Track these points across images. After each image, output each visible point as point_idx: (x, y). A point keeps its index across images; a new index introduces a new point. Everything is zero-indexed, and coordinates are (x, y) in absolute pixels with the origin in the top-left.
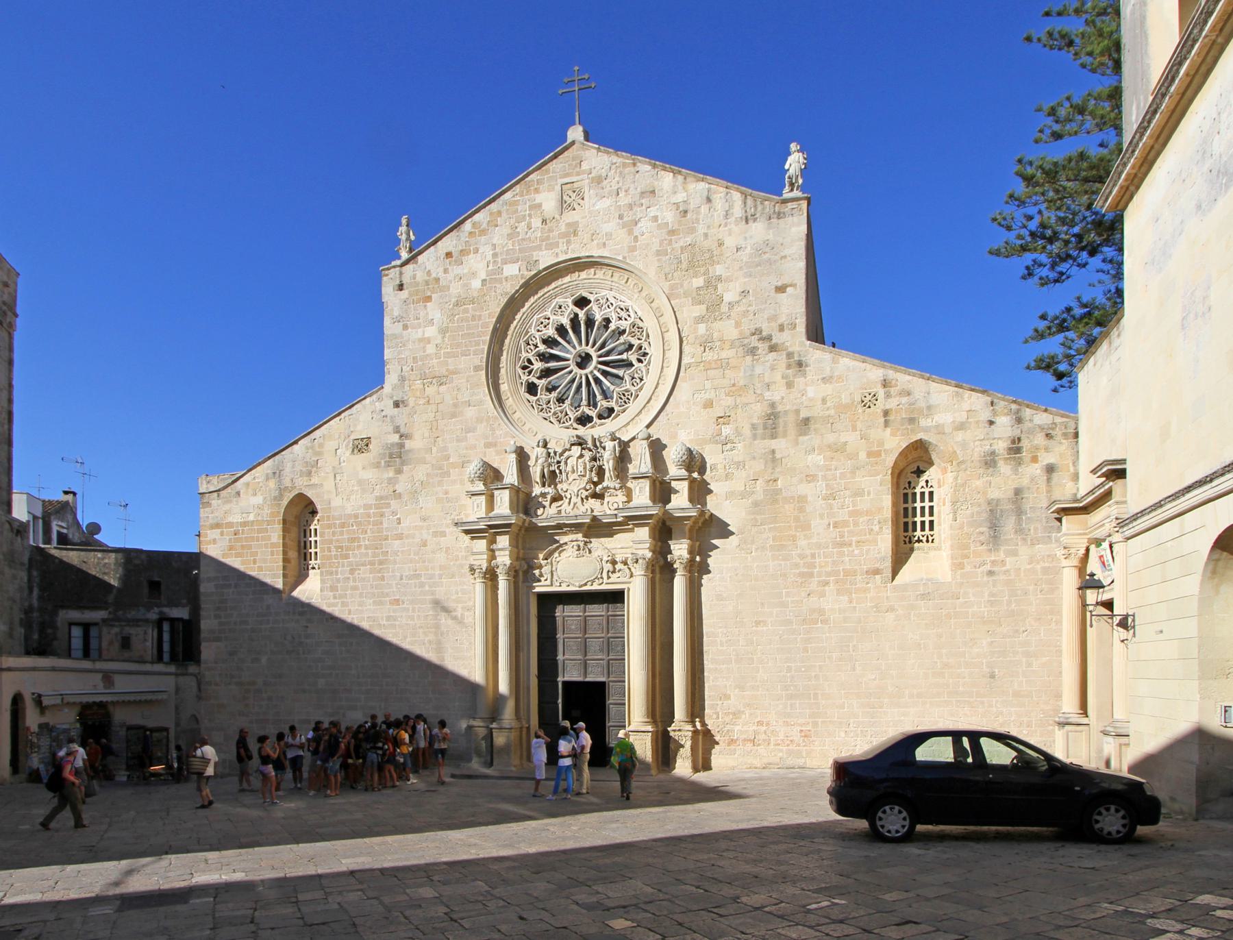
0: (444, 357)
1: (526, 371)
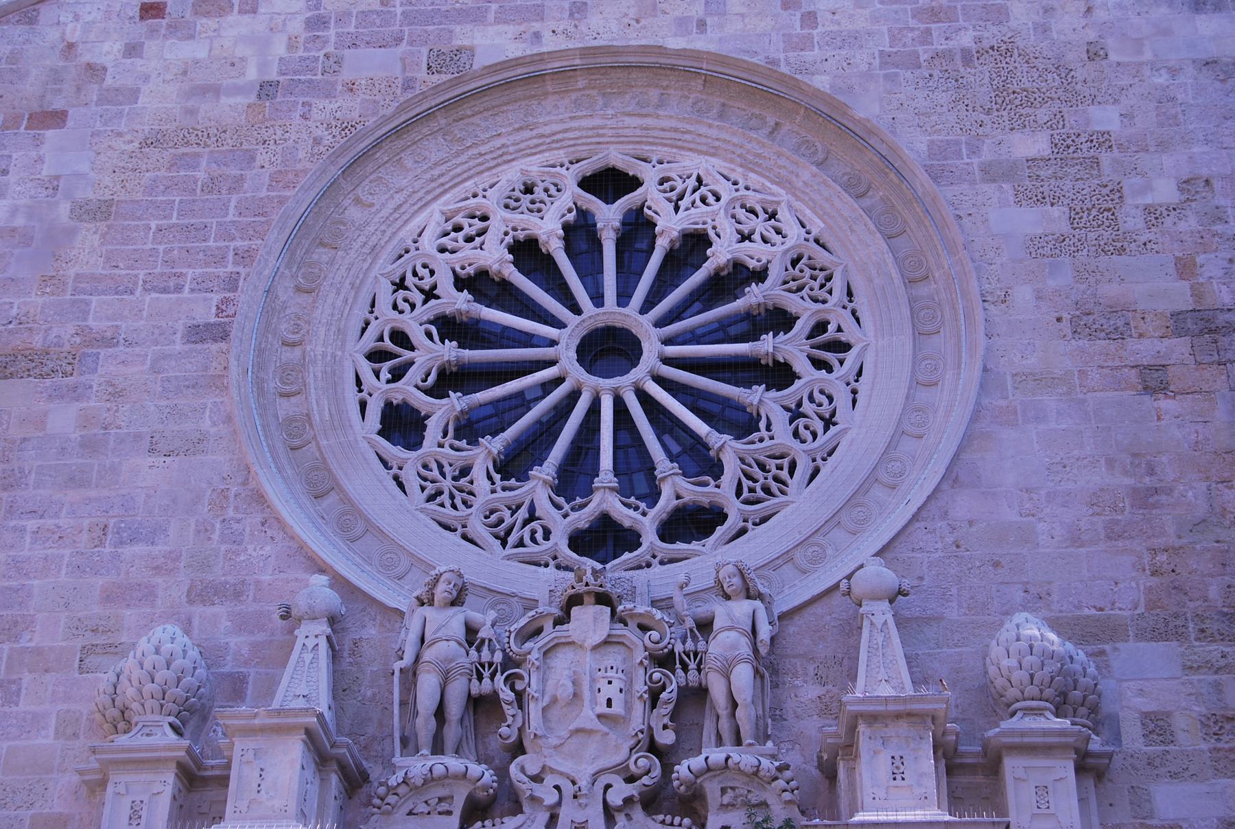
0: (76, 291)
1: (386, 367)
